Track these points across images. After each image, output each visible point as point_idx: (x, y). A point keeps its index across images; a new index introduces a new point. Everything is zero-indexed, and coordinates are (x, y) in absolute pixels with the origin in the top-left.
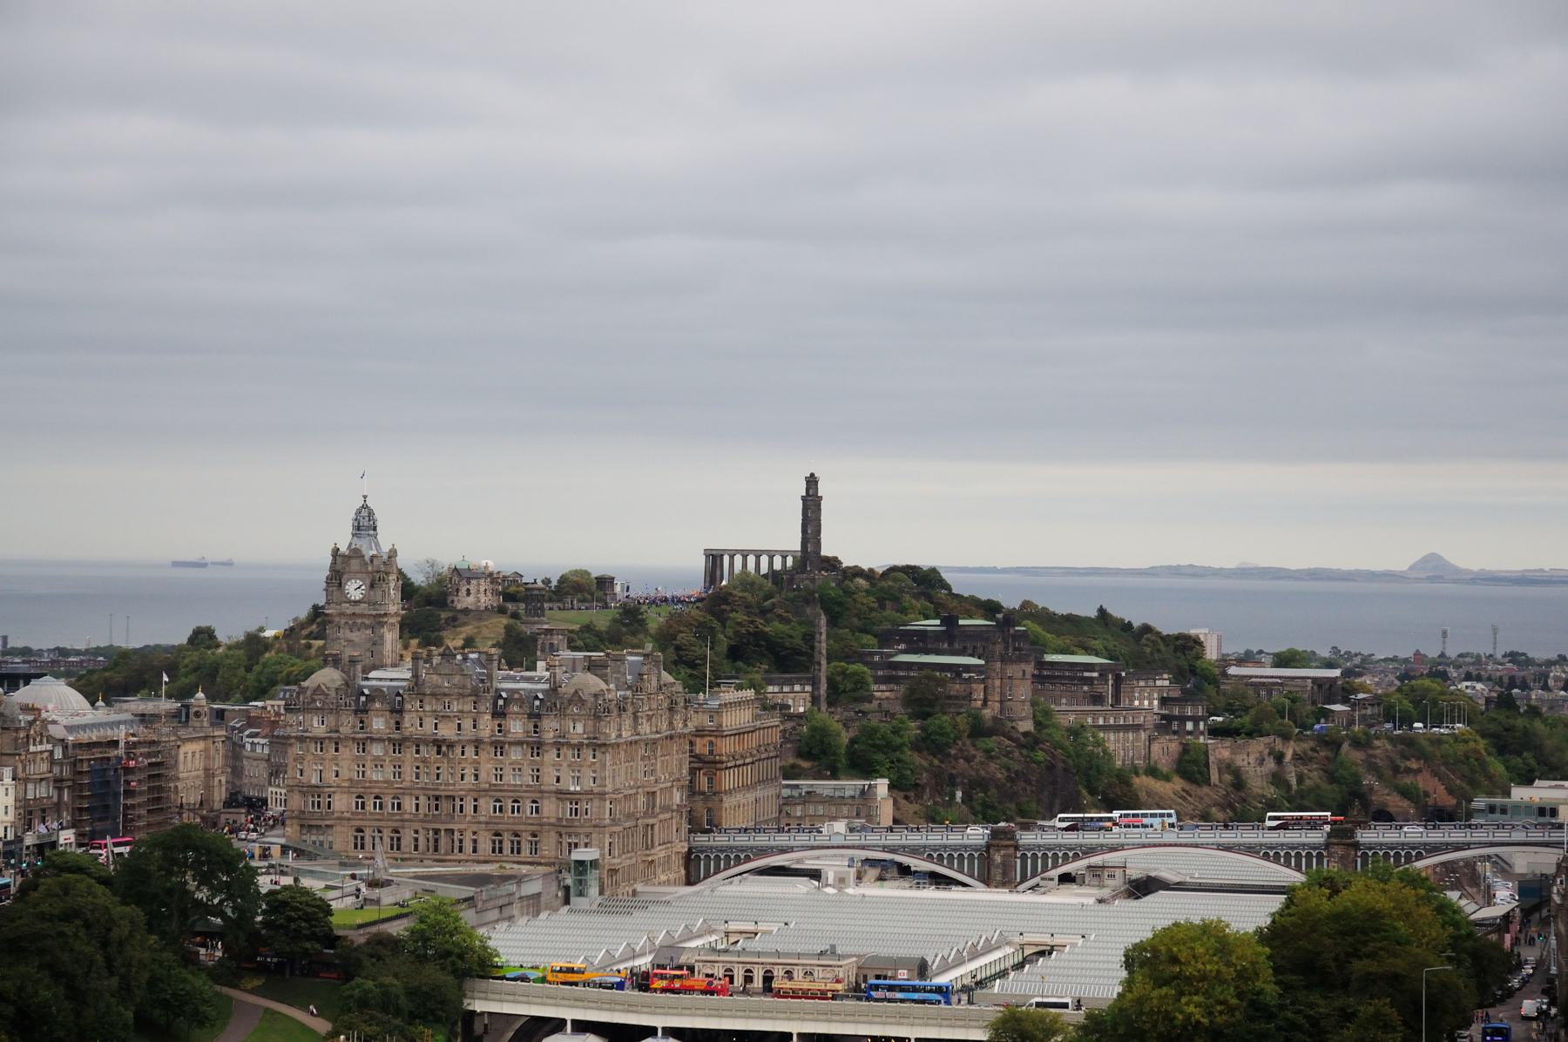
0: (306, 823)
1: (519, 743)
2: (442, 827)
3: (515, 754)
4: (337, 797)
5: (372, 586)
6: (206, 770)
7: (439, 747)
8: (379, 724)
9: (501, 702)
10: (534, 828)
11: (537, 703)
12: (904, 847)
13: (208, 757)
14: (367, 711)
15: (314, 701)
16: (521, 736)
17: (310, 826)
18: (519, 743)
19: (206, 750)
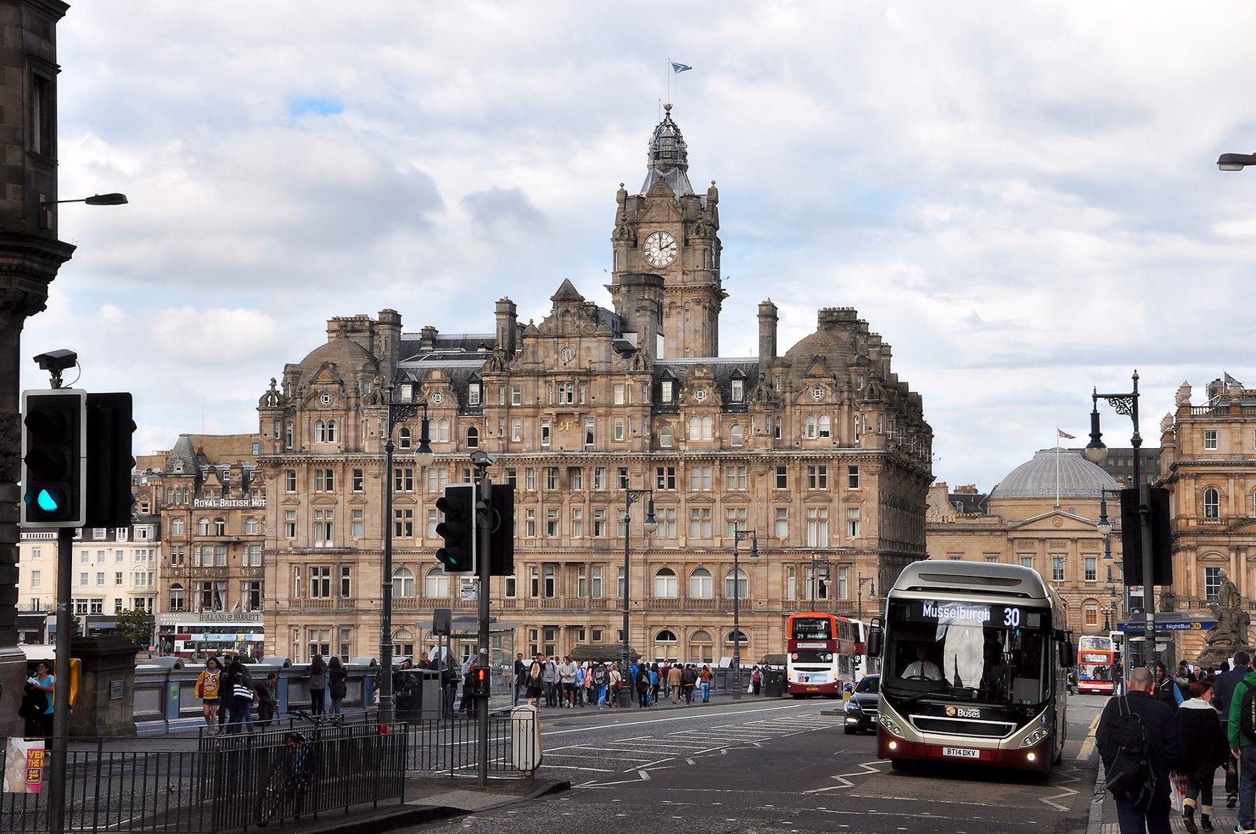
1: (707, 460)
2: (564, 621)
3: (702, 480)
9: (667, 388)
11: (737, 385)
18: (707, 460)
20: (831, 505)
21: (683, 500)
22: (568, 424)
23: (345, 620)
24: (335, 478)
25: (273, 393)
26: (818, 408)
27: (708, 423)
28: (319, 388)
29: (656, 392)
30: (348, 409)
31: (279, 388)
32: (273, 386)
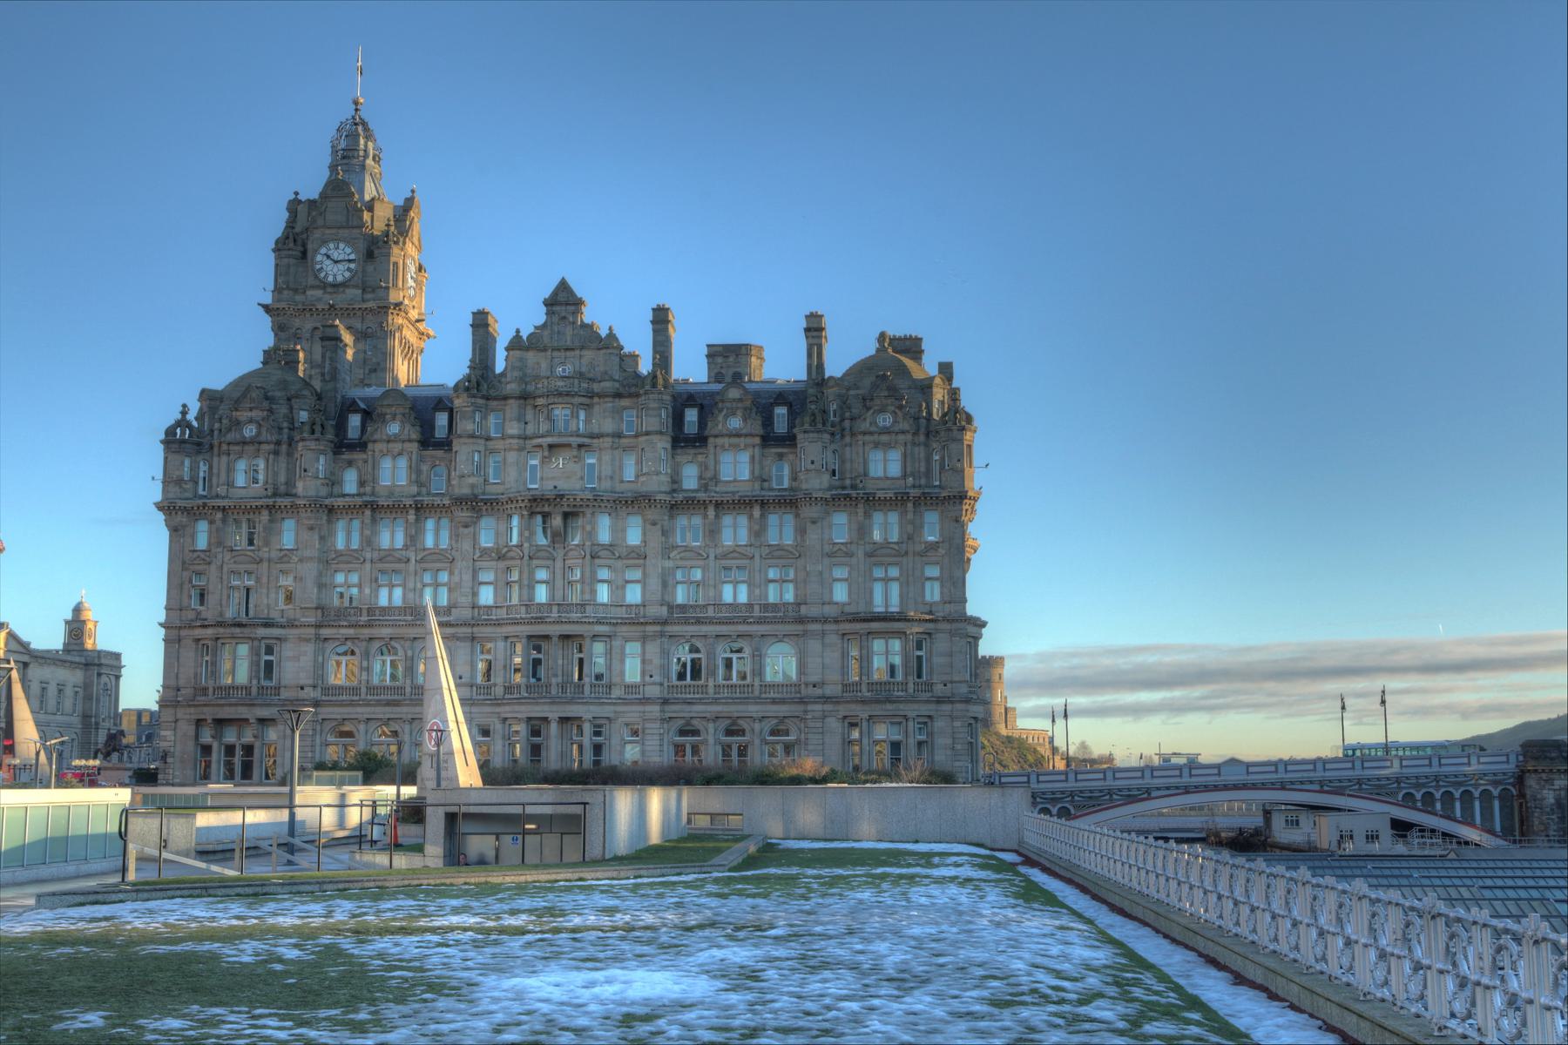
0: (209, 714)
2: (553, 713)
4: (288, 650)
5: (370, 255)
6: (86, 717)
7: (546, 516)
8: (394, 473)
9: (691, 415)
10: (783, 710)
11: (781, 411)
12: (1359, 782)
13: (88, 698)
14: (361, 445)
15: (237, 424)
16: (746, 490)
17: (220, 723)
18: (742, 504)
19: (87, 686)
20: (905, 560)
21: (712, 557)
22: (560, 462)
23: (265, 713)
24: (259, 528)
25: (182, 423)
26: (884, 438)
27: (744, 457)
28: (243, 415)
29: (678, 419)
30: (278, 443)
31: (191, 416)
32: (184, 413)
